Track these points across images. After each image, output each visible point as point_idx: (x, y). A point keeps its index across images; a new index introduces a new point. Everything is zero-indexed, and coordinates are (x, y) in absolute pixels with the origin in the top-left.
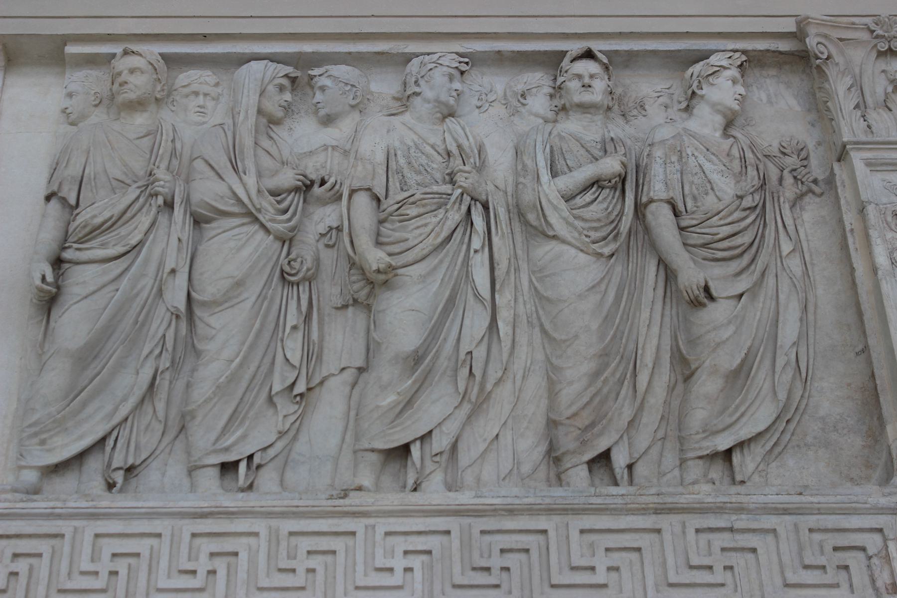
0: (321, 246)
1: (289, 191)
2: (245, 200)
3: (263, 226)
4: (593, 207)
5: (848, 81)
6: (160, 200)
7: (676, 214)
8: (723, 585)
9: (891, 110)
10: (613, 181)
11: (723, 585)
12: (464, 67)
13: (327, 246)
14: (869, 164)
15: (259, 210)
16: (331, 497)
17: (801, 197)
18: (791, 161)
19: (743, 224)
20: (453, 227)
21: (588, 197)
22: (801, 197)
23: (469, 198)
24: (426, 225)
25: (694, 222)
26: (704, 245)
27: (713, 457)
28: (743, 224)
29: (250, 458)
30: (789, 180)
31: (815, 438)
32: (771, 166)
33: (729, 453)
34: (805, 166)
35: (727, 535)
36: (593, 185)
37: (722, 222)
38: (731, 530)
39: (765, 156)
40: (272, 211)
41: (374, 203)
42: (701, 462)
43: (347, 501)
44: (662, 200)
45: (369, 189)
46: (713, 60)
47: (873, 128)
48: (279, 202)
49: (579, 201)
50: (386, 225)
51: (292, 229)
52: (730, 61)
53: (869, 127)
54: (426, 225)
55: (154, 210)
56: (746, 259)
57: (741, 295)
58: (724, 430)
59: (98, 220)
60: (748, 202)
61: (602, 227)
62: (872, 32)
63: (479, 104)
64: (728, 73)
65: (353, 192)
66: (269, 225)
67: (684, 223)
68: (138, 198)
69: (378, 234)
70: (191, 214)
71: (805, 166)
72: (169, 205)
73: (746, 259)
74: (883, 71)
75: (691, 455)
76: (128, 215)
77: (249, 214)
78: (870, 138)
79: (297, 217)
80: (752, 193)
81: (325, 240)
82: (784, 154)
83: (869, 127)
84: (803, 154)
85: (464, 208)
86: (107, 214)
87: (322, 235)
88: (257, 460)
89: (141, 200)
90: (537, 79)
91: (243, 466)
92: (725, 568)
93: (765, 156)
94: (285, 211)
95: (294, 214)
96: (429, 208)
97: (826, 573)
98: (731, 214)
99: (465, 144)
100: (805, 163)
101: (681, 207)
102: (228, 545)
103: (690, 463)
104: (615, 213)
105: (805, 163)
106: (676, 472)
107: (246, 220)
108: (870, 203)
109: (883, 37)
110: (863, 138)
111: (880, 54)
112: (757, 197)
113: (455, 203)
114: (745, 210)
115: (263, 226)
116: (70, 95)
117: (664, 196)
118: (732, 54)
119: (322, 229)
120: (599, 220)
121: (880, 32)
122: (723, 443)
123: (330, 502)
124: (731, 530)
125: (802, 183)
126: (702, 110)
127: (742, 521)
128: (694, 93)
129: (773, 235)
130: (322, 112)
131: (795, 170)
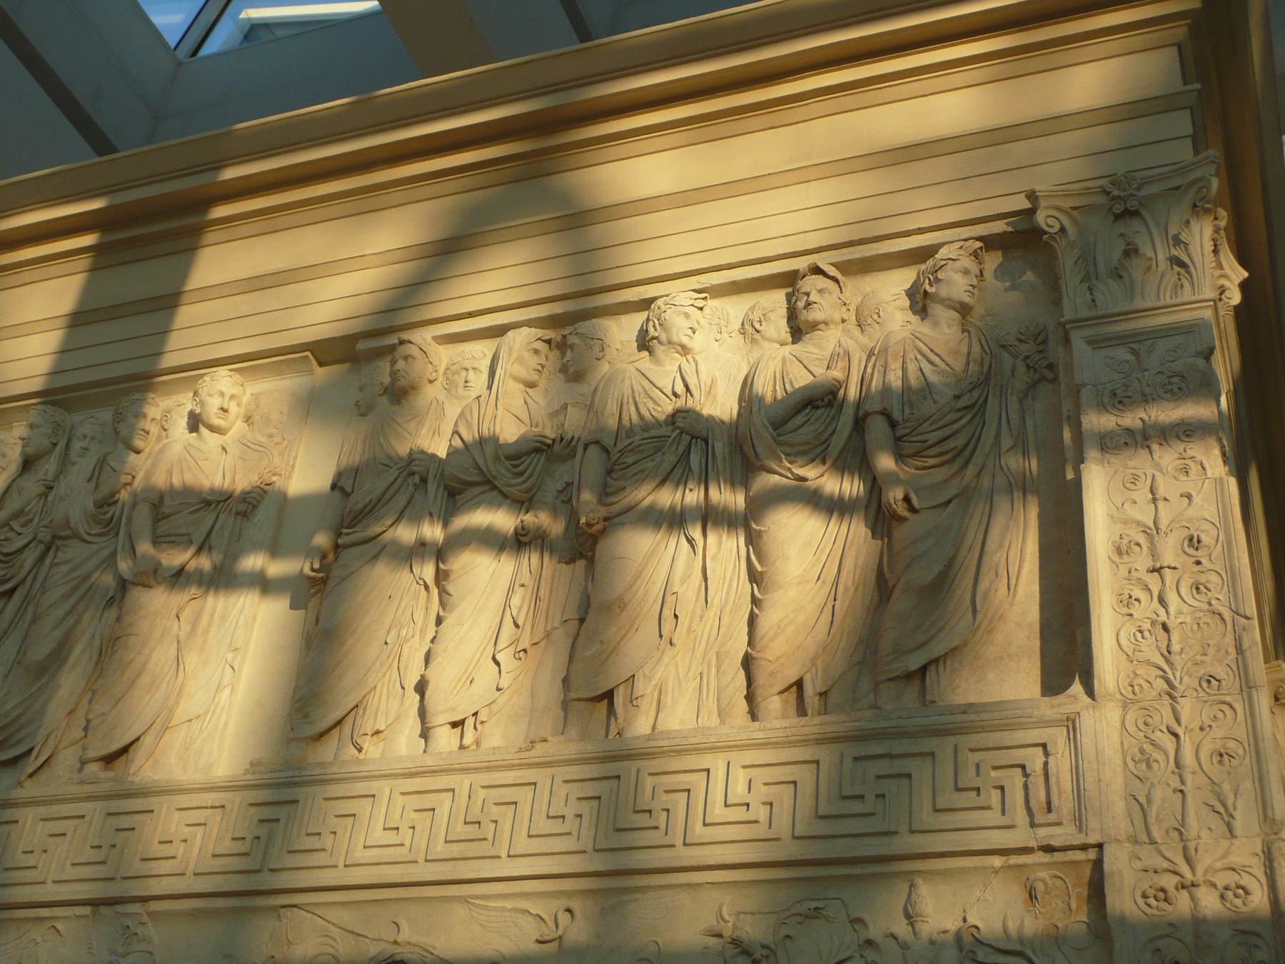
0: (558, 502)
1: (528, 453)
2: (484, 469)
3: (501, 492)
4: (802, 431)
5: (1077, 253)
6: (417, 479)
7: (893, 424)
8: (873, 814)
9: (1121, 277)
10: (826, 400)
11: (873, 814)
12: (700, 303)
13: (563, 502)
14: (1090, 341)
15: (495, 478)
16: (520, 750)
17: (1034, 385)
18: (1025, 349)
19: (956, 426)
20: (669, 469)
21: (800, 419)
22: (1034, 385)
23: (688, 438)
24: (642, 471)
25: (907, 431)
26: (917, 454)
27: (908, 676)
28: (956, 426)
29: (475, 714)
30: (1021, 368)
31: (1019, 647)
32: (1006, 355)
33: (923, 670)
34: (1040, 352)
35: (886, 762)
36: (805, 407)
37: (933, 427)
38: (889, 756)
39: (1003, 346)
40: (509, 475)
41: (604, 455)
42: (892, 684)
43: (533, 753)
44: (875, 413)
45: (597, 442)
46: (943, 253)
47: (1098, 303)
48: (515, 466)
49: (791, 425)
50: (614, 476)
51: (528, 491)
52: (961, 252)
53: (1093, 301)
54: (642, 471)
55: (411, 489)
56: (955, 467)
57: (949, 502)
58: (913, 650)
59: (360, 505)
60: (962, 403)
61: (811, 449)
62: (1108, 193)
63: (718, 336)
64: (958, 264)
65: (586, 447)
66: (505, 489)
67: (900, 432)
68: (395, 480)
69: (606, 485)
70: (446, 487)
71: (1040, 352)
72: (424, 481)
73: (959, 461)
74: (1122, 235)
75: (882, 678)
76: (387, 496)
77: (488, 482)
78: (1093, 313)
79: (534, 478)
80: (970, 391)
81: (562, 497)
82: (1020, 341)
83: (1093, 301)
84: (1041, 338)
85: (681, 449)
86: (367, 500)
87: (560, 492)
88: (481, 717)
89: (399, 481)
90: (776, 300)
91: (470, 723)
92: (878, 796)
93: (1003, 346)
94: (521, 474)
95: (530, 476)
96: (646, 453)
97: (979, 795)
98: (944, 416)
99: (692, 383)
100: (1042, 347)
101: (897, 415)
102: (427, 801)
103: (881, 686)
104: (828, 432)
105: (1042, 347)
106: (871, 697)
107: (486, 487)
108: (1085, 385)
109: (1119, 197)
110: (1085, 313)
111: (1117, 217)
112: (976, 394)
113: (672, 444)
114: (960, 410)
115: (501, 492)
116: (361, 389)
117: (877, 407)
118: (961, 243)
119: (560, 486)
120: (807, 443)
121: (1116, 193)
122: (914, 663)
123: (517, 756)
124: (889, 756)
125: (1035, 371)
126: (937, 310)
127: (898, 747)
128: (925, 292)
129: (993, 432)
130: (571, 370)
131: (1028, 357)
